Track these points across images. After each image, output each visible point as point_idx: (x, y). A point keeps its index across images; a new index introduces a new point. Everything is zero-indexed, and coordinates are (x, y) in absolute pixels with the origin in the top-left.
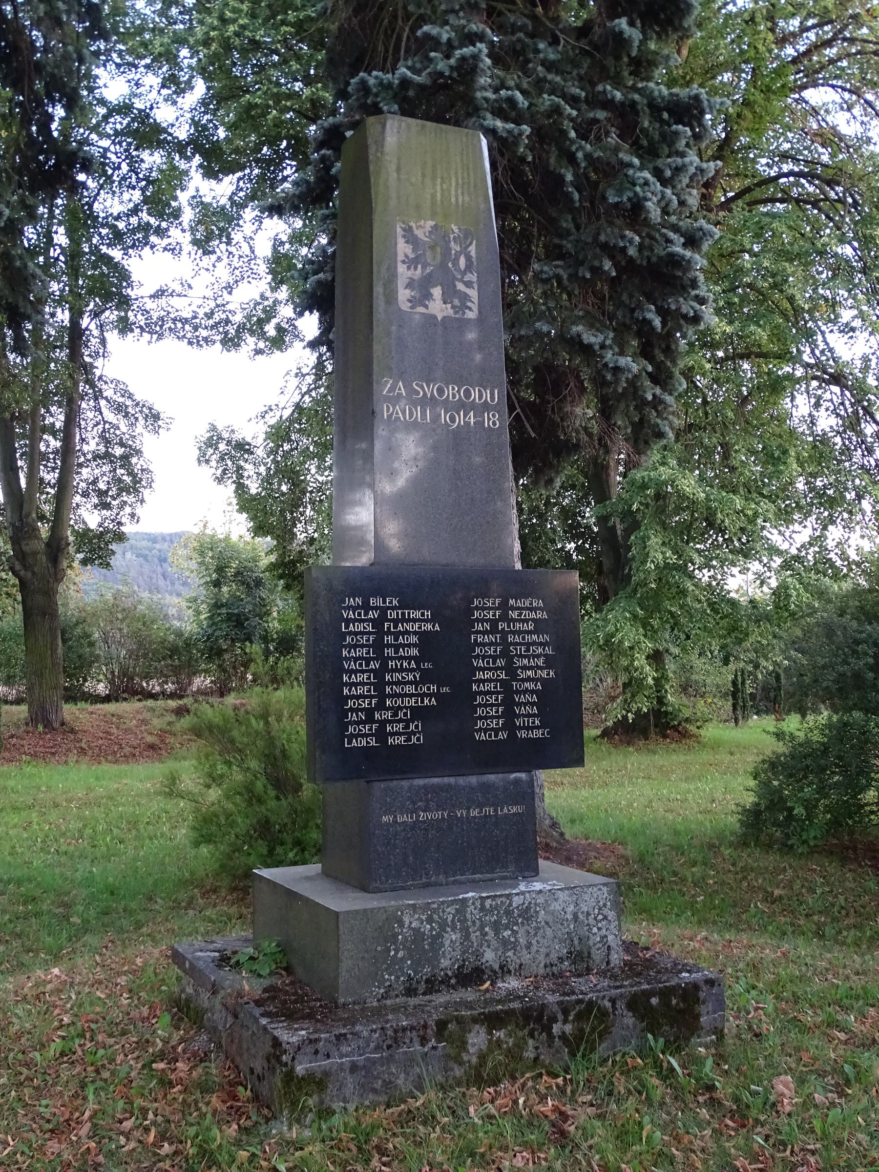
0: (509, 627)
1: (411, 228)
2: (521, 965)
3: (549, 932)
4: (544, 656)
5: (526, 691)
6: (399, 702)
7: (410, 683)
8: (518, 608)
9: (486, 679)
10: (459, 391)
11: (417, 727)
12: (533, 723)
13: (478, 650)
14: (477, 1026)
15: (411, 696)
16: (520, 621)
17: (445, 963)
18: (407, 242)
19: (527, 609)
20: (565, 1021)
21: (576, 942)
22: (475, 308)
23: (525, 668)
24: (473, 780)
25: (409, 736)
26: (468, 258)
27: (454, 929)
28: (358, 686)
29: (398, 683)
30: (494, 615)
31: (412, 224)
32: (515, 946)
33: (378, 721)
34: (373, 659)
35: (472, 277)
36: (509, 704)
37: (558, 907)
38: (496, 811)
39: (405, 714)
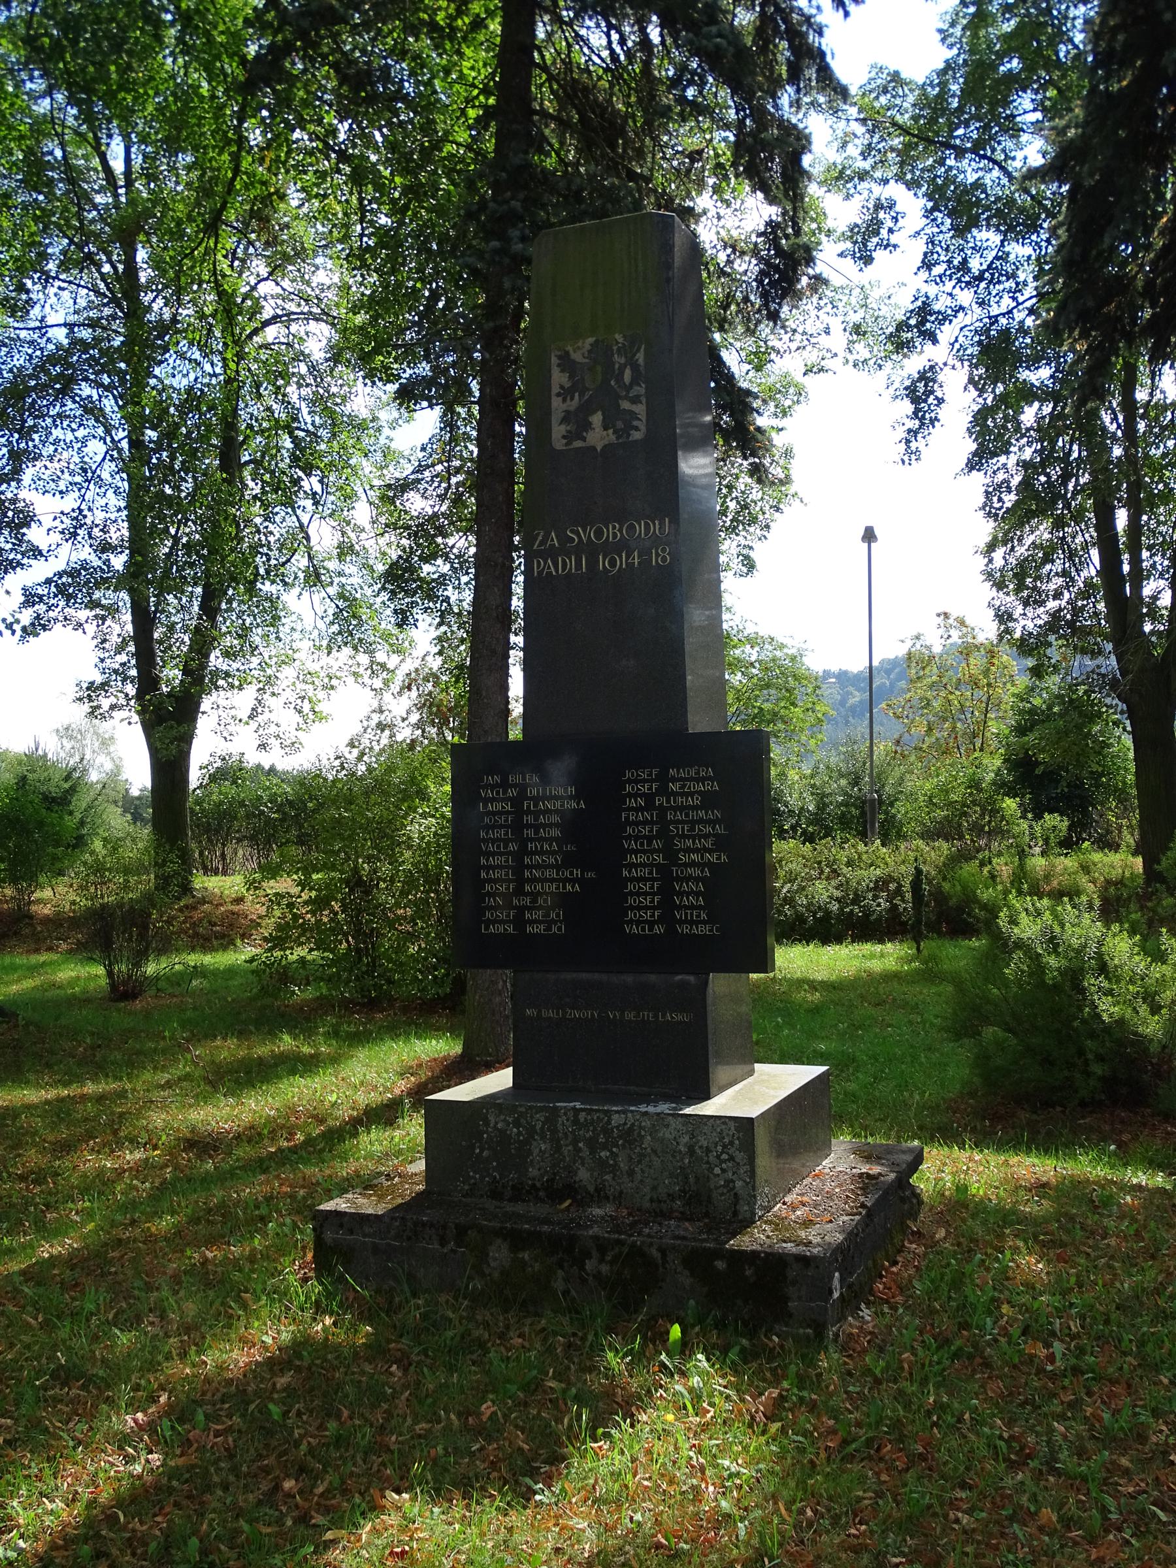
0: (668, 801)
1: (567, 353)
2: (621, 1192)
3: (657, 1162)
4: (714, 835)
5: (689, 879)
6: (539, 887)
7: (551, 866)
8: (681, 779)
9: (640, 863)
10: (620, 530)
11: (558, 915)
12: (699, 916)
13: (629, 830)
14: (499, 1241)
15: (552, 880)
16: (682, 794)
17: (533, 1172)
18: (562, 371)
19: (691, 779)
20: (602, 1261)
21: (692, 1180)
22: (643, 428)
23: (688, 851)
24: (629, 979)
25: (549, 924)
26: (635, 367)
27: (543, 1138)
28: (497, 872)
29: (538, 867)
30: (650, 788)
31: (569, 348)
32: (614, 1169)
33: (516, 907)
34: (511, 840)
35: (640, 390)
36: (667, 892)
37: (667, 1135)
38: (656, 1016)
39: (546, 901)
